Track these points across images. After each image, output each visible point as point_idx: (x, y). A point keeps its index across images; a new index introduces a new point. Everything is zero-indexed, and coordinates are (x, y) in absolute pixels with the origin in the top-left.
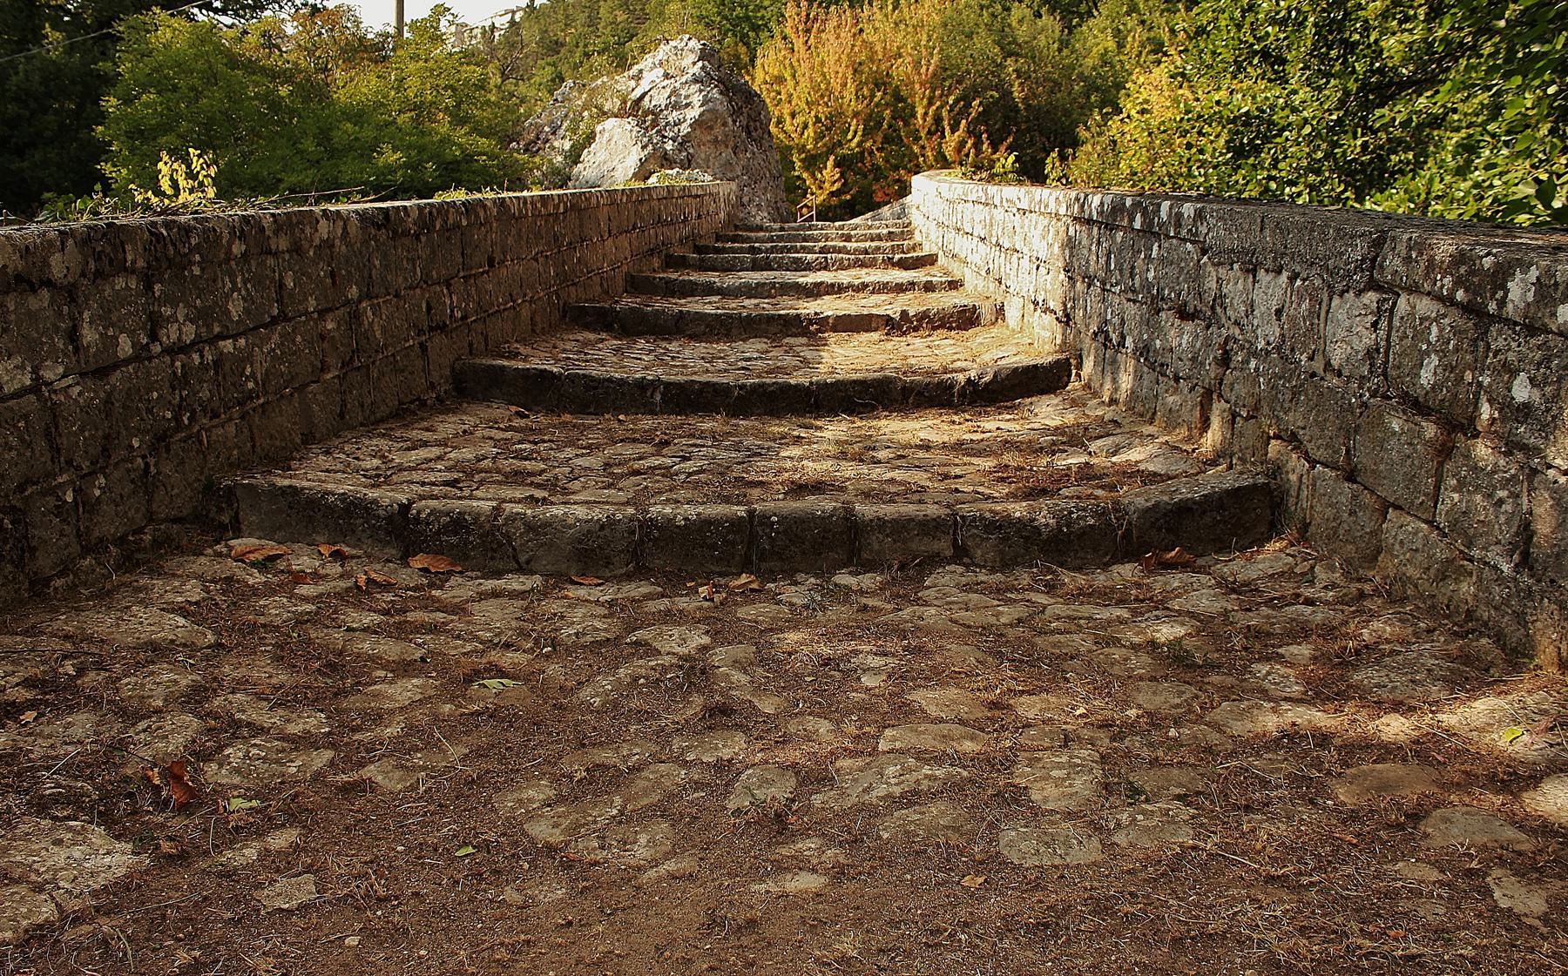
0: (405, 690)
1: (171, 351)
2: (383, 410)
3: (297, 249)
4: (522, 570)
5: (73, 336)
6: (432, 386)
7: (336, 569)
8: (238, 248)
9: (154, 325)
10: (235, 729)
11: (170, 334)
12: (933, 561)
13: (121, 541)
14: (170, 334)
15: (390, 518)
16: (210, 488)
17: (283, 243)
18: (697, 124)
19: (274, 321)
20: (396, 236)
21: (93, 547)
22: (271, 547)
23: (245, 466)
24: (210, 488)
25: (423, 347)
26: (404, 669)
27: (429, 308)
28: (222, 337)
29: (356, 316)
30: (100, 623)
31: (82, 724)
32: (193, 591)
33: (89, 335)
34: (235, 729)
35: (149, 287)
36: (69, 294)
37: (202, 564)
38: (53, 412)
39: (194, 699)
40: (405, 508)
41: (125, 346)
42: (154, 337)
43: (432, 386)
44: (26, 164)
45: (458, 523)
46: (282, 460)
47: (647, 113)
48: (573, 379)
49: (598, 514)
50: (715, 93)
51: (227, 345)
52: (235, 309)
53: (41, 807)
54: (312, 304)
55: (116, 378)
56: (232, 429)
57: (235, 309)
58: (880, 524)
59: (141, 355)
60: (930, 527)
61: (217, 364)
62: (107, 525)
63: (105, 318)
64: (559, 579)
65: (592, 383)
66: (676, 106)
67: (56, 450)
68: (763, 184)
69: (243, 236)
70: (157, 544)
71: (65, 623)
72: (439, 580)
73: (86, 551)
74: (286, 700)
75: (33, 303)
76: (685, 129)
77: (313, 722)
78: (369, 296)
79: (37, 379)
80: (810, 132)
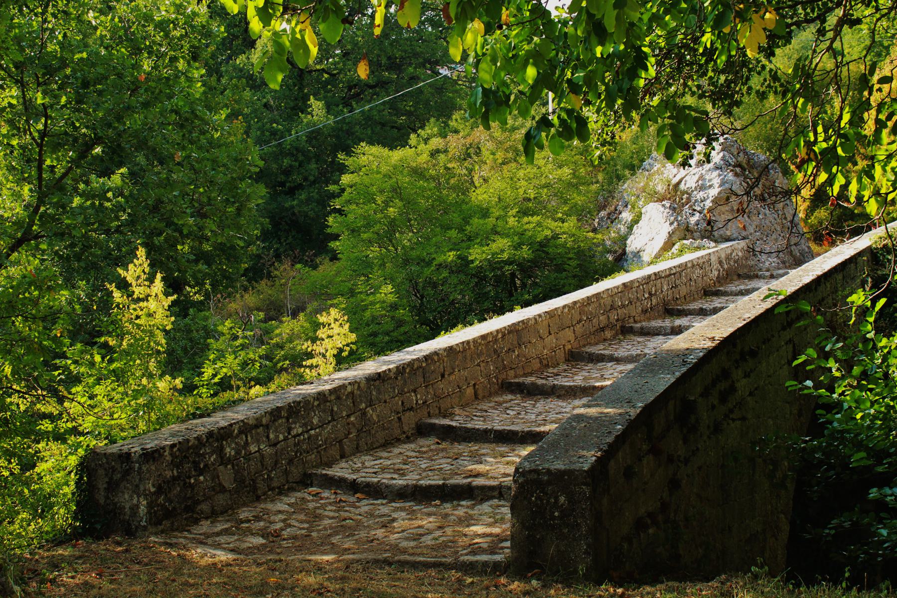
1: (294, 437)
2: (377, 444)
3: (338, 398)
4: (384, 498)
5: (268, 437)
6: (404, 433)
7: (333, 496)
8: (316, 403)
9: (289, 430)
10: (290, 526)
11: (294, 432)
12: (492, 498)
13: (279, 488)
14: (294, 432)
15: (351, 483)
17: (333, 397)
18: (716, 201)
19: (329, 422)
20: (384, 381)
21: (272, 489)
22: (319, 490)
23: (317, 467)
25: (399, 419)
27: (403, 403)
28: (311, 429)
29: (364, 414)
30: (270, 506)
31: (262, 524)
32: (293, 500)
33: (272, 436)
34: (290, 526)
35: (288, 420)
36: (267, 427)
37: (299, 494)
38: (262, 456)
39: (284, 521)
40: (355, 480)
41: (281, 437)
42: (289, 434)
43: (404, 433)
44: (295, 202)
45: (368, 485)
46: (329, 465)
47: (683, 193)
48: (460, 428)
49: (405, 483)
50: (730, 176)
51: (313, 432)
52: (315, 421)
53: (252, 534)
54: (344, 414)
55: (278, 446)
56: (313, 456)
57: (315, 421)
59: (286, 439)
61: (309, 438)
62: (275, 484)
63: (276, 431)
66: (702, 188)
67: (262, 465)
68: (774, 236)
69: (318, 399)
70: (289, 489)
71: (262, 506)
72: (359, 500)
73: (269, 490)
74: (302, 522)
75: (259, 431)
76: (708, 204)
77: (306, 525)
78: (371, 406)
79: (259, 449)
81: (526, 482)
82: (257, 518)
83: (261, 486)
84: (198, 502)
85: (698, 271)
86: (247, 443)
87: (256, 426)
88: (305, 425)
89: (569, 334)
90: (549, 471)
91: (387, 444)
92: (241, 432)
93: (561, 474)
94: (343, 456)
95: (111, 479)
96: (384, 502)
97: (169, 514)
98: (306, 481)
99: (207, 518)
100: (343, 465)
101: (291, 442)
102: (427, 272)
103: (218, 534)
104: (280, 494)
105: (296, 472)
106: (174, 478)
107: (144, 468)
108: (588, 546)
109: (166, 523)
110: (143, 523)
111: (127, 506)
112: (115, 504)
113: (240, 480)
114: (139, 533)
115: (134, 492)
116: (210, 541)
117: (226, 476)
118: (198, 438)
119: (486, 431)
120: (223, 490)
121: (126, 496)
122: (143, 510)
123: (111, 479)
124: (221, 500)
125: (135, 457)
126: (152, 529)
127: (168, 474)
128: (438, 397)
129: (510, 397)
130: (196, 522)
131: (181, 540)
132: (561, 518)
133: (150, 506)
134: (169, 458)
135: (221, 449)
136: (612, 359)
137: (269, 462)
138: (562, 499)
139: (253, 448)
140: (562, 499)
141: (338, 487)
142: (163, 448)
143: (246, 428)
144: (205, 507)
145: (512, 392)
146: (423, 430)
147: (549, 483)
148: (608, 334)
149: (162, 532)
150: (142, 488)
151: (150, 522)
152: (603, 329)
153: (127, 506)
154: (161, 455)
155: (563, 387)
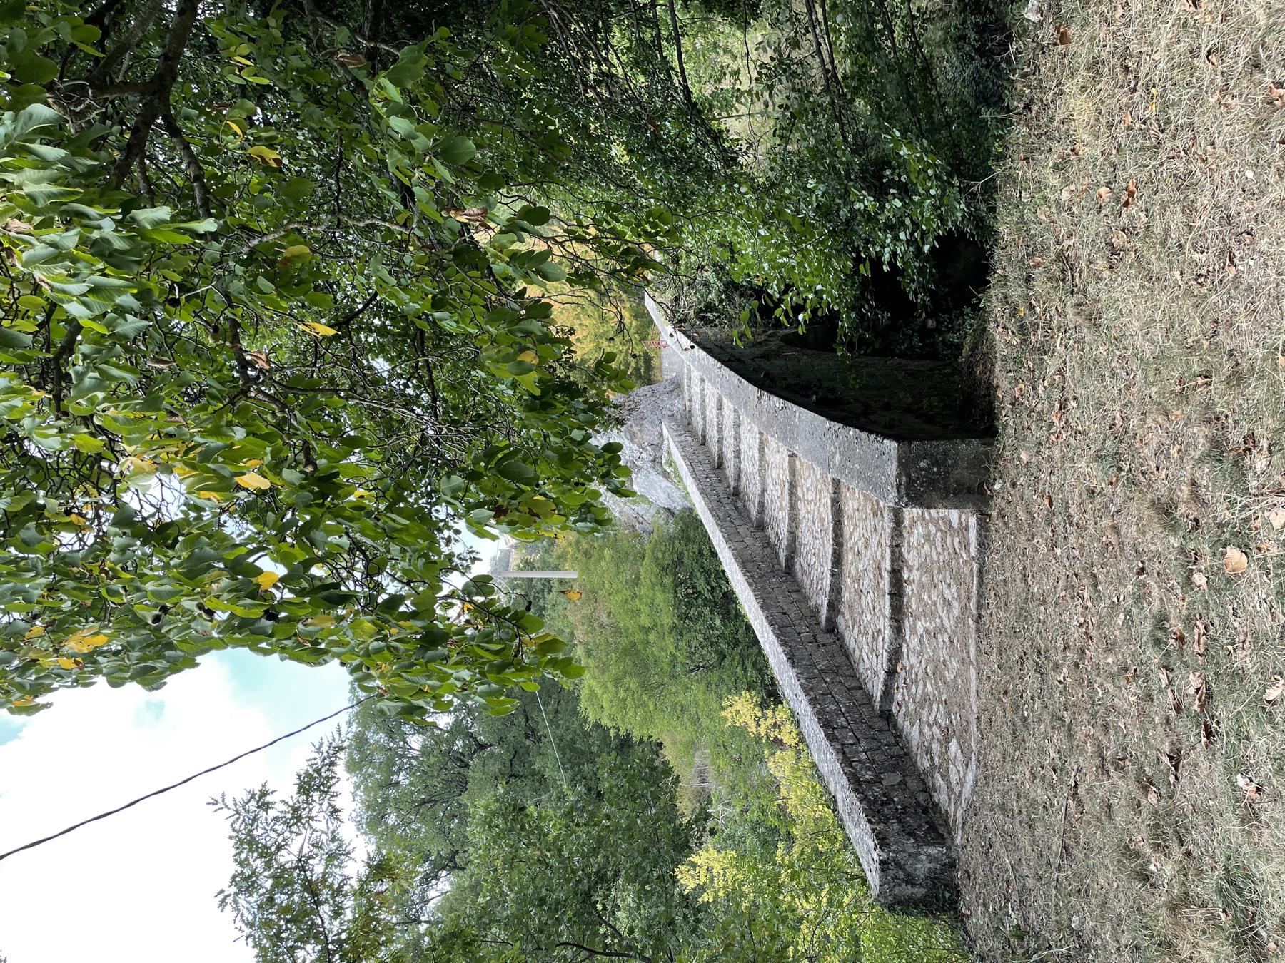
0: (929, 689)
3: (812, 689)
4: (901, 646)
9: (843, 727)
10: (935, 720)
11: (845, 724)
12: (900, 553)
14: (845, 724)
16: (880, 716)
21: (897, 743)
22: (895, 704)
24: (880, 716)
26: (925, 685)
30: (914, 743)
31: (934, 746)
32: (908, 723)
34: (935, 720)
36: (843, 745)
37: (900, 720)
38: (869, 749)
39: (930, 727)
45: (890, 661)
46: (870, 698)
49: (888, 628)
52: (834, 707)
57: (834, 707)
58: (892, 565)
59: (852, 730)
60: (893, 553)
62: (893, 740)
64: (903, 639)
65: (832, 590)
71: (915, 749)
72: (903, 667)
74: (931, 711)
76: (635, 447)
77: (935, 706)
80: (587, 322)
81: (907, 495)
82: (929, 751)
83: (895, 751)
84: (918, 803)
85: (688, 448)
86: (860, 761)
87: (844, 753)
88: (837, 715)
89: (742, 530)
90: (899, 476)
91: (846, 654)
92: (851, 766)
93: (900, 464)
94: (861, 688)
95: (903, 880)
96: (904, 645)
97: (932, 828)
98: (887, 716)
99: (931, 796)
100: (869, 685)
101: (854, 727)
102: (680, 659)
103: (949, 783)
104: (900, 737)
105: (880, 724)
106: (899, 821)
107: (894, 847)
108: (963, 442)
109: (941, 830)
110: (944, 850)
111: (929, 865)
112: (927, 878)
113: (894, 768)
114: (954, 855)
115: (915, 858)
116: (957, 790)
117: (891, 779)
118: (861, 801)
119: (833, 575)
120: (903, 782)
121: (919, 866)
122: (933, 851)
123: (903, 880)
124: (913, 784)
125: (884, 856)
126: (949, 843)
127: (896, 827)
128: (803, 617)
129: (797, 567)
130: (936, 805)
131: (959, 814)
132: (938, 466)
133: (928, 844)
134: (882, 826)
135: (867, 782)
136: (762, 495)
137: (874, 744)
138: (922, 464)
139: (863, 756)
140: (922, 464)
141: (892, 687)
142: (874, 830)
143: (846, 761)
144: (921, 797)
145: (793, 565)
146: (832, 628)
147: (908, 476)
148: (740, 504)
149: (950, 834)
150: (912, 850)
151: (942, 844)
152: (736, 508)
153: (929, 865)
154: (880, 833)
155: (789, 525)
